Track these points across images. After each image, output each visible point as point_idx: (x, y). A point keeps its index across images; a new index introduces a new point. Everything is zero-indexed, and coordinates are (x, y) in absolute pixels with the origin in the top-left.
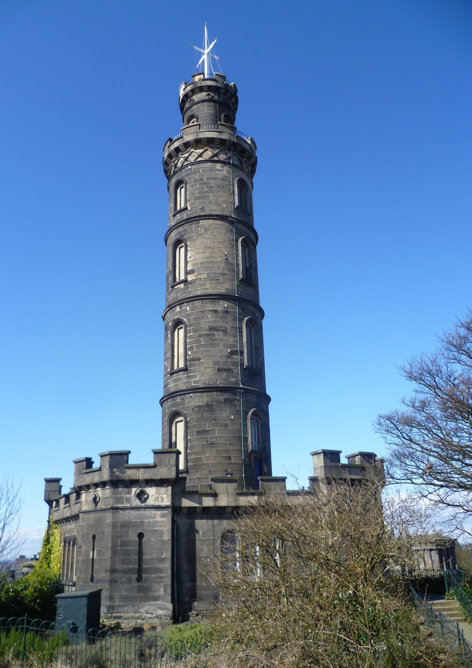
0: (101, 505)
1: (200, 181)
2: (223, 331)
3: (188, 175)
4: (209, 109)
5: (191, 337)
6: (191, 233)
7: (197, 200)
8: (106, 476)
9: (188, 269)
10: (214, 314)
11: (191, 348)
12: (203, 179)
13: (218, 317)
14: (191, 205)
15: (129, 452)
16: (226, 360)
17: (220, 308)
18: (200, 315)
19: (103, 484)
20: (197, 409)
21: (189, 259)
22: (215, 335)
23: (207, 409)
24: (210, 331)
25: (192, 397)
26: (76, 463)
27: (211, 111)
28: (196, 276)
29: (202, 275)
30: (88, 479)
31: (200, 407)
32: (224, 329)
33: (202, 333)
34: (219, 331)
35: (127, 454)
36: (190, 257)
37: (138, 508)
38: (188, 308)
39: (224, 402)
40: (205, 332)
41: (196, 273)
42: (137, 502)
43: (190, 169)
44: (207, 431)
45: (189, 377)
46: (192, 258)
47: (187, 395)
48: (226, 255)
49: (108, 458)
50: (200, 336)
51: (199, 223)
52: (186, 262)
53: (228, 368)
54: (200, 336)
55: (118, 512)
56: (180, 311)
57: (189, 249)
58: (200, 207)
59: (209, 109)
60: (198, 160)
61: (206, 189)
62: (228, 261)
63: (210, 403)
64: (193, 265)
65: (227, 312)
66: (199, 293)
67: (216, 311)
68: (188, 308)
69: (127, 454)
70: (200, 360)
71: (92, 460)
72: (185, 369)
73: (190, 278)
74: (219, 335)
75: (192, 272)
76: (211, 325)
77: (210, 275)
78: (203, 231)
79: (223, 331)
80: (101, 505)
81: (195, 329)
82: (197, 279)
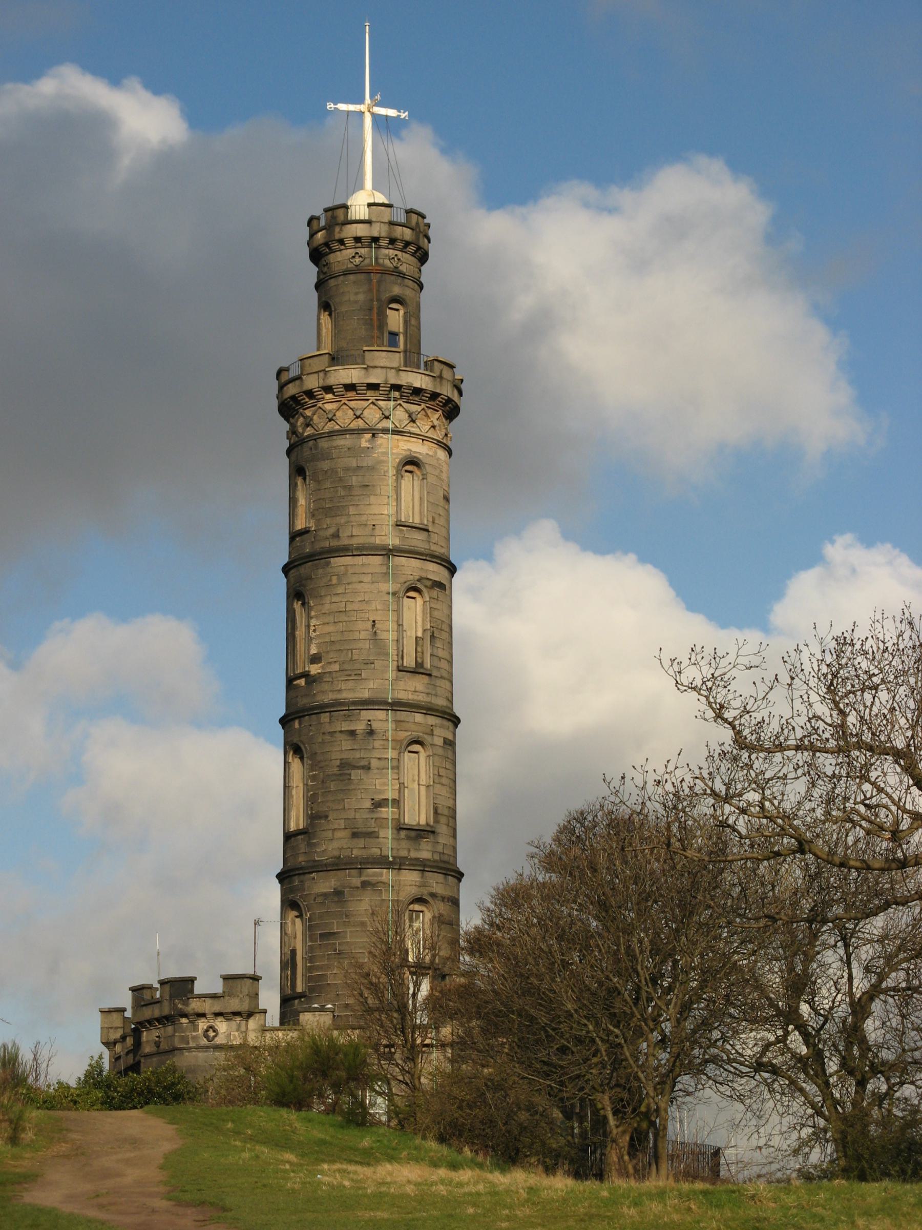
2: (363, 768)
17: (360, 727)
22: (350, 775)
23: (336, 899)
27: (361, 297)
28: (322, 667)
30: (148, 1013)
32: (366, 763)
35: (192, 980)
36: (314, 631)
37: (207, 1048)
39: (362, 887)
42: (204, 1042)
44: (335, 933)
47: (307, 876)
55: (183, 1054)
59: (356, 294)
63: (339, 889)
64: (319, 645)
65: (371, 732)
67: (352, 733)
69: (192, 980)
71: (126, 1000)
75: (315, 659)
79: (363, 768)
82: (324, 673)
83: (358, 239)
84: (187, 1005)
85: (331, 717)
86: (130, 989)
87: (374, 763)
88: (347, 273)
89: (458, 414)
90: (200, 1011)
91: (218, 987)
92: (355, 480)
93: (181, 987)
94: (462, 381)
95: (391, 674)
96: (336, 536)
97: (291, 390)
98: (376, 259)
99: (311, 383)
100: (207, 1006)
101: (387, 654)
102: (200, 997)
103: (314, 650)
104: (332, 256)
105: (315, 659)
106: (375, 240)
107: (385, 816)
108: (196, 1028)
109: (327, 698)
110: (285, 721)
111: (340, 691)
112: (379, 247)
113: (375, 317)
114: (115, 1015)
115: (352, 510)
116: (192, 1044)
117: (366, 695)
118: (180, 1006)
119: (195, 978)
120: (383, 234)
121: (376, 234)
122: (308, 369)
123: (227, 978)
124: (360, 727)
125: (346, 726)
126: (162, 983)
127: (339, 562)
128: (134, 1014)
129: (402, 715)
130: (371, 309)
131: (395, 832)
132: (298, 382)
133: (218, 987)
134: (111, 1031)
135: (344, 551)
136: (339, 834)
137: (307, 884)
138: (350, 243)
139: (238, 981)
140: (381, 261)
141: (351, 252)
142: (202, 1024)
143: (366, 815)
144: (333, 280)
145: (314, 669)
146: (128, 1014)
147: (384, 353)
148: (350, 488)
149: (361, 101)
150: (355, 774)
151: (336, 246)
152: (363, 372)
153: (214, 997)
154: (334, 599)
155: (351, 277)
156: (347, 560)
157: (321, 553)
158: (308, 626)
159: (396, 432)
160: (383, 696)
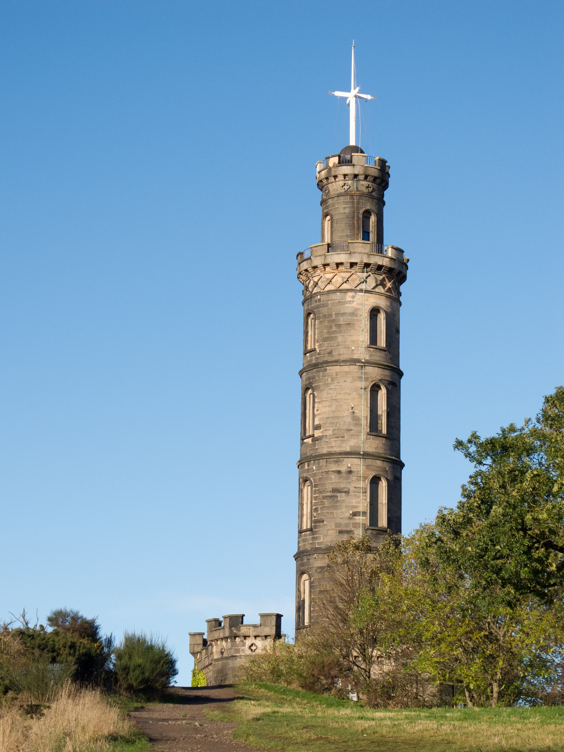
0: (225, 655)
1: (328, 317)
2: (345, 492)
3: (317, 307)
4: (345, 208)
5: (316, 498)
6: (318, 382)
7: (325, 341)
8: (227, 634)
9: (315, 424)
10: (338, 475)
11: (316, 510)
12: (332, 315)
13: (341, 478)
14: (320, 346)
15: (244, 615)
16: (347, 521)
17: (343, 469)
18: (325, 475)
19: (226, 638)
20: (319, 570)
21: (316, 413)
22: (337, 497)
24: (333, 492)
25: (315, 558)
26: (208, 622)
27: (347, 211)
28: (322, 432)
29: (328, 431)
30: (217, 635)
31: (322, 568)
32: (347, 490)
33: (325, 495)
34: (342, 492)
36: (317, 410)
38: (314, 468)
40: (329, 494)
41: (322, 430)
43: (319, 300)
45: (314, 539)
46: (319, 412)
48: (352, 408)
49: (228, 620)
50: (324, 497)
51: (326, 370)
52: (314, 416)
53: (349, 529)
54: (324, 497)
56: (308, 469)
57: (316, 400)
58: (328, 351)
59: (345, 208)
60: (327, 289)
61: (334, 329)
62: (355, 415)
64: (320, 420)
65: (350, 472)
66: (325, 451)
67: (339, 472)
68: (314, 468)
70: (323, 522)
72: (311, 530)
73: (317, 433)
74: (342, 497)
75: (317, 427)
76: (334, 486)
77: (336, 432)
78: (330, 380)
79: (345, 492)
80: (225, 655)
81: (320, 491)
83: (345, 176)
84: (239, 631)
85: (327, 462)
86: (208, 621)
87: (352, 489)
88: (339, 196)
89: (405, 280)
90: (247, 635)
91: (257, 620)
92: (342, 320)
93: (236, 621)
94: (408, 260)
95: (363, 436)
96: (330, 353)
97: (305, 266)
98: (357, 188)
99: (318, 262)
100: (252, 632)
101: (361, 425)
102: (247, 626)
103: (317, 422)
104: (330, 185)
105: (317, 427)
106: (356, 176)
107: (357, 521)
108: (244, 645)
109: (325, 450)
110: (301, 464)
111: (332, 447)
112: (359, 180)
113: (356, 223)
114: (198, 637)
115: (340, 339)
116: (242, 654)
117: (348, 449)
118: (235, 631)
119: (282, 616)
120: (361, 172)
121: (357, 173)
122: (314, 253)
123: (263, 616)
124: (343, 469)
125: (334, 467)
126: (225, 618)
127: (332, 370)
128: (208, 636)
129: (369, 461)
130: (353, 218)
131: (364, 531)
132: (309, 261)
133: (257, 620)
134: (196, 646)
135: (336, 362)
136: (330, 532)
137: (311, 561)
138: (341, 178)
139: (269, 617)
140: (360, 189)
141: (341, 183)
142: (248, 642)
143: (347, 521)
144: (330, 200)
145: (317, 433)
146: (205, 637)
147: (361, 244)
148: (339, 326)
149: (349, 91)
150: (341, 497)
151: (332, 179)
152: (348, 255)
153: (255, 626)
154: (329, 391)
155: (342, 198)
156: (337, 368)
157: (322, 363)
158: (314, 407)
159: (367, 291)
160: (358, 450)
